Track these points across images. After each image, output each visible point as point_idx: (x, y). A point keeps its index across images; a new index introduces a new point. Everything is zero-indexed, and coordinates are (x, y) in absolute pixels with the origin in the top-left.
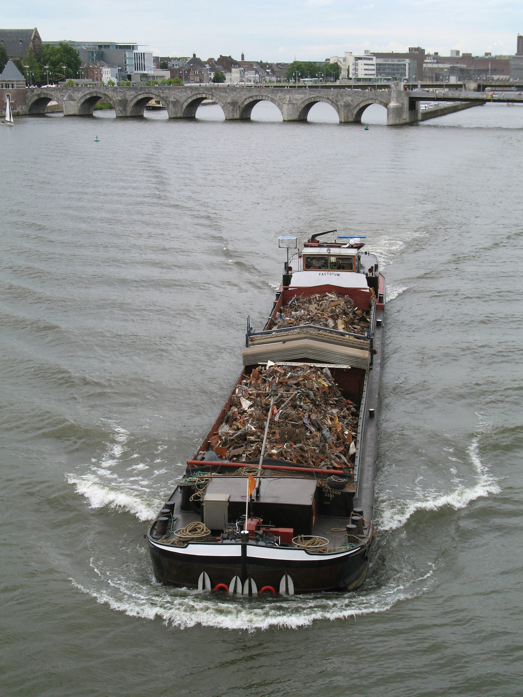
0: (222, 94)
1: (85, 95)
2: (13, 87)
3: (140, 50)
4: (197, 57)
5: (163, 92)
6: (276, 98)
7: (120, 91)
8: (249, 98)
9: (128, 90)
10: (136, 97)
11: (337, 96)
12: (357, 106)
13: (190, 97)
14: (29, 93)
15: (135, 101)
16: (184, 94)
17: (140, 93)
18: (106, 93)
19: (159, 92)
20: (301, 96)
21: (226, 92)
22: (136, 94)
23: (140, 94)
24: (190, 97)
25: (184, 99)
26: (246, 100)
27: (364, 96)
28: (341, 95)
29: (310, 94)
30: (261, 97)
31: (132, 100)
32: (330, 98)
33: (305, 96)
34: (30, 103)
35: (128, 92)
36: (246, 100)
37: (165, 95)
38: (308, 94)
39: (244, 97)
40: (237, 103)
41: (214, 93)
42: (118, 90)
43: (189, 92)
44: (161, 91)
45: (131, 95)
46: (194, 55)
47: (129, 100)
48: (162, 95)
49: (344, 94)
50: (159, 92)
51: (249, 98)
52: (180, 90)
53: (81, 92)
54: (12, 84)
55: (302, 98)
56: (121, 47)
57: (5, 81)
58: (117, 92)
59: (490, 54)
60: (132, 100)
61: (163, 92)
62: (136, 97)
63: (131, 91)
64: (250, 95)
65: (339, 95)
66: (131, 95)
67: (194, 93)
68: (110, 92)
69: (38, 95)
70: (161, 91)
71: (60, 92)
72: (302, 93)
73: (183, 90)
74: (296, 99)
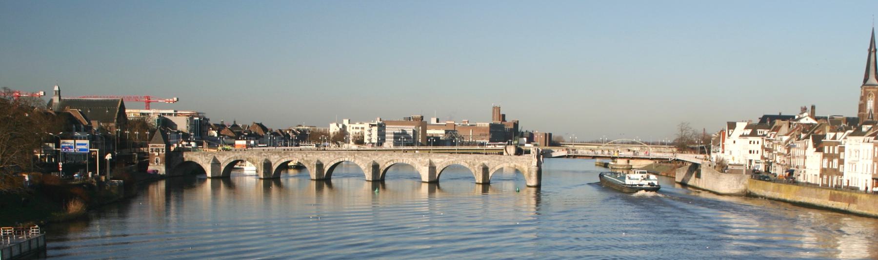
0: (364, 158)
1: (230, 159)
2: (163, 152)
7: (264, 156)
8: (390, 161)
9: (272, 155)
10: (280, 160)
11: (475, 160)
12: (493, 169)
15: (226, 164)
16: (328, 158)
19: (302, 156)
20: (442, 160)
21: (368, 157)
22: (280, 158)
23: (283, 158)
24: (332, 161)
26: (387, 163)
27: (499, 160)
28: (478, 159)
29: (449, 158)
30: (396, 161)
31: (275, 163)
32: (468, 161)
33: (444, 160)
35: (272, 156)
36: (387, 163)
37: (308, 159)
38: (447, 159)
39: (385, 161)
41: (357, 157)
42: (263, 154)
43: (332, 156)
44: (305, 155)
45: (275, 159)
46: (235, 122)
48: (305, 159)
49: (481, 158)
50: (302, 156)
51: (390, 161)
52: (323, 155)
53: (225, 156)
54: (162, 149)
55: (442, 162)
58: (261, 156)
60: (275, 163)
61: (306, 156)
62: (280, 160)
63: (275, 155)
64: (391, 159)
65: (476, 160)
66: (275, 159)
68: (255, 156)
70: (305, 155)
71: (205, 156)
72: (441, 157)
73: (327, 154)
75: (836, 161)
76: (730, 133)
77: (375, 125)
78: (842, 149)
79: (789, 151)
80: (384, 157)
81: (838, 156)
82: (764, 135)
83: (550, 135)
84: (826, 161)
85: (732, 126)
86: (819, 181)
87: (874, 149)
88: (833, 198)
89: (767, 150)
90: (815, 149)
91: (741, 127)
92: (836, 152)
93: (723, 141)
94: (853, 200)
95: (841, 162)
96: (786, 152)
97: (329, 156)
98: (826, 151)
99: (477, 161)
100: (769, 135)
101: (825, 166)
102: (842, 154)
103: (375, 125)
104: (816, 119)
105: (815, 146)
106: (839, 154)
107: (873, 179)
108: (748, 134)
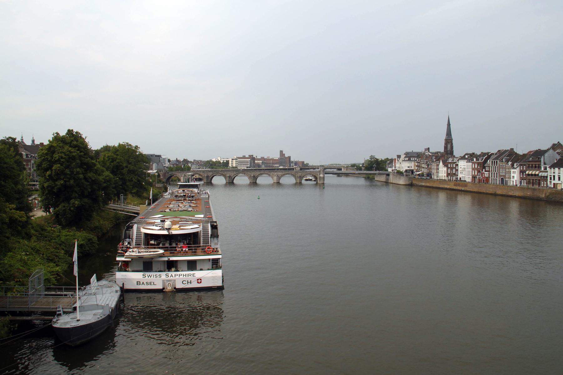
3: (163, 157)
4: (178, 159)
5: (224, 173)
6: (271, 174)
10: (213, 174)
11: (295, 173)
13: (235, 174)
14: (167, 174)
17: (214, 173)
18: (200, 173)
20: (281, 173)
22: (212, 174)
23: (214, 174)
24: (235, 174)
25: (232, 175)
32: (293, 174)
34: (167, 178)
37: (225, 174)
39: (258, 174)
40: (255, 176)
43: (235, 172)
46: (177, 159)
47: (209, 176)
56: (156, 156)
57: (159, 169)
59: (269, 157)
62: (213, 174)
67: (237, 173)
69: (171, 174)
71: (180, 173)
72: (282, 172)
74: (279, 174)
75: (454, 170)
76: (398, 160)
77: (234, 159)
78: (457, 165)
79: (428, 166)
80: (257, 173)
81: (455, 168)
82: (415, 160)
83: (304, 162)
84: (449, 170)
85: (399, 157)
86: (446, 178)
87: (472, 165)
88: (455, 185)
89: (417, 166)
90: (444, 166)
91: (403, 157)
92: (454, 166)
93: (395, 163)
94: (466, 186)
95: (457, 170)
96: (427, 167)
97: (233, 172)
98: (449, 166)
99: (296, 174)
100: (417, 160)
101: (449, 172)
102: (457, 167)
103: (234, 159)
104: (431, 153)
105: (443, 164)
106: (456, 167)
107: (472, 177)
108: (407, 159)
